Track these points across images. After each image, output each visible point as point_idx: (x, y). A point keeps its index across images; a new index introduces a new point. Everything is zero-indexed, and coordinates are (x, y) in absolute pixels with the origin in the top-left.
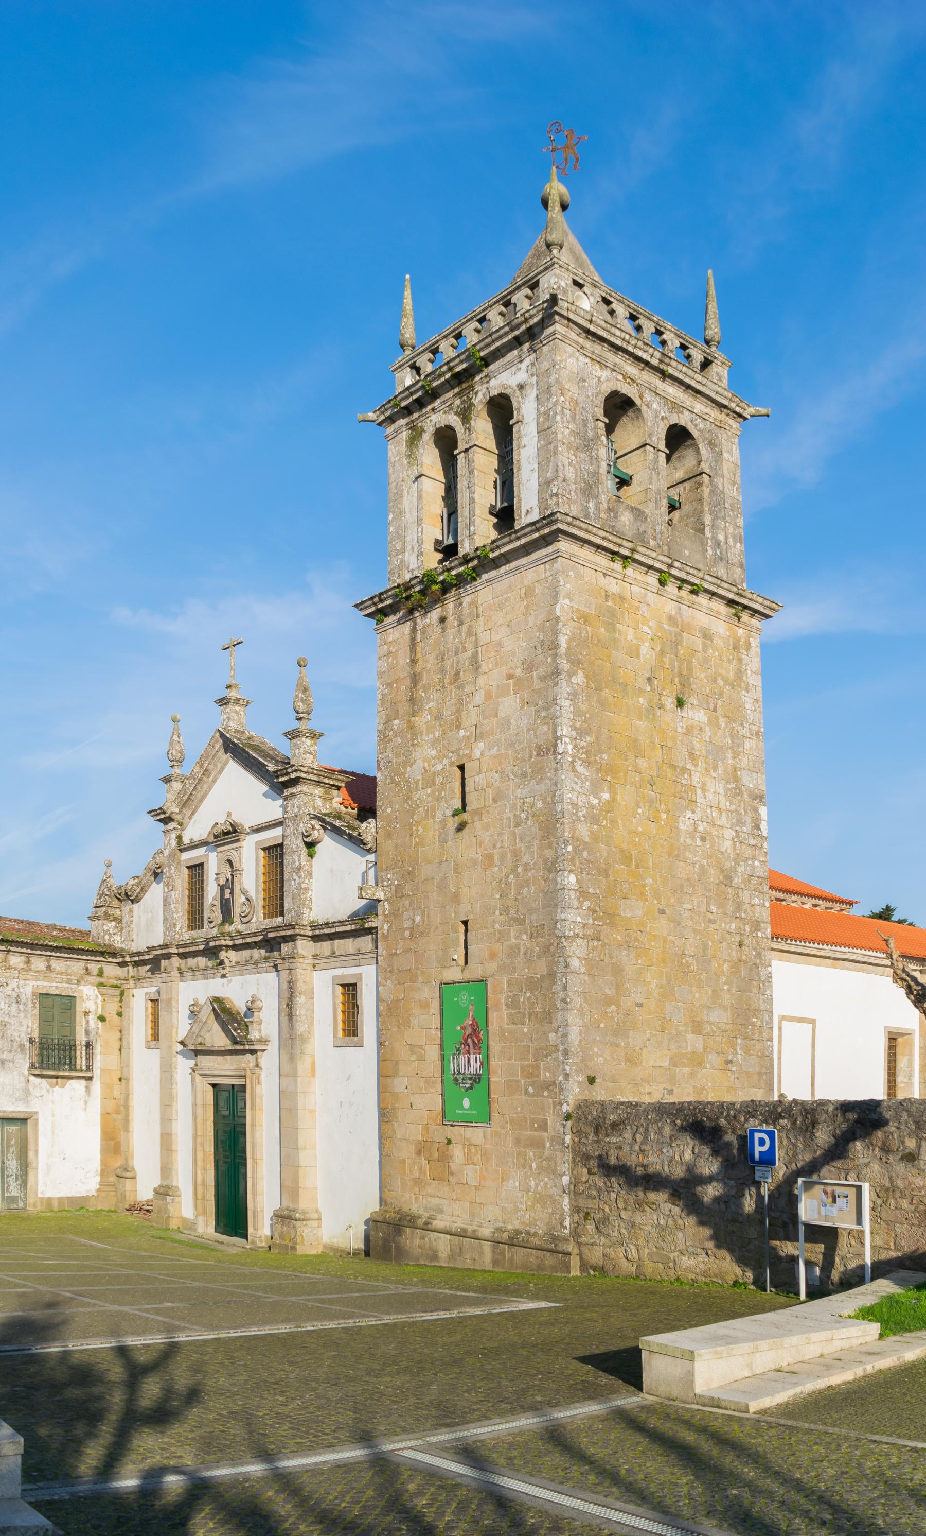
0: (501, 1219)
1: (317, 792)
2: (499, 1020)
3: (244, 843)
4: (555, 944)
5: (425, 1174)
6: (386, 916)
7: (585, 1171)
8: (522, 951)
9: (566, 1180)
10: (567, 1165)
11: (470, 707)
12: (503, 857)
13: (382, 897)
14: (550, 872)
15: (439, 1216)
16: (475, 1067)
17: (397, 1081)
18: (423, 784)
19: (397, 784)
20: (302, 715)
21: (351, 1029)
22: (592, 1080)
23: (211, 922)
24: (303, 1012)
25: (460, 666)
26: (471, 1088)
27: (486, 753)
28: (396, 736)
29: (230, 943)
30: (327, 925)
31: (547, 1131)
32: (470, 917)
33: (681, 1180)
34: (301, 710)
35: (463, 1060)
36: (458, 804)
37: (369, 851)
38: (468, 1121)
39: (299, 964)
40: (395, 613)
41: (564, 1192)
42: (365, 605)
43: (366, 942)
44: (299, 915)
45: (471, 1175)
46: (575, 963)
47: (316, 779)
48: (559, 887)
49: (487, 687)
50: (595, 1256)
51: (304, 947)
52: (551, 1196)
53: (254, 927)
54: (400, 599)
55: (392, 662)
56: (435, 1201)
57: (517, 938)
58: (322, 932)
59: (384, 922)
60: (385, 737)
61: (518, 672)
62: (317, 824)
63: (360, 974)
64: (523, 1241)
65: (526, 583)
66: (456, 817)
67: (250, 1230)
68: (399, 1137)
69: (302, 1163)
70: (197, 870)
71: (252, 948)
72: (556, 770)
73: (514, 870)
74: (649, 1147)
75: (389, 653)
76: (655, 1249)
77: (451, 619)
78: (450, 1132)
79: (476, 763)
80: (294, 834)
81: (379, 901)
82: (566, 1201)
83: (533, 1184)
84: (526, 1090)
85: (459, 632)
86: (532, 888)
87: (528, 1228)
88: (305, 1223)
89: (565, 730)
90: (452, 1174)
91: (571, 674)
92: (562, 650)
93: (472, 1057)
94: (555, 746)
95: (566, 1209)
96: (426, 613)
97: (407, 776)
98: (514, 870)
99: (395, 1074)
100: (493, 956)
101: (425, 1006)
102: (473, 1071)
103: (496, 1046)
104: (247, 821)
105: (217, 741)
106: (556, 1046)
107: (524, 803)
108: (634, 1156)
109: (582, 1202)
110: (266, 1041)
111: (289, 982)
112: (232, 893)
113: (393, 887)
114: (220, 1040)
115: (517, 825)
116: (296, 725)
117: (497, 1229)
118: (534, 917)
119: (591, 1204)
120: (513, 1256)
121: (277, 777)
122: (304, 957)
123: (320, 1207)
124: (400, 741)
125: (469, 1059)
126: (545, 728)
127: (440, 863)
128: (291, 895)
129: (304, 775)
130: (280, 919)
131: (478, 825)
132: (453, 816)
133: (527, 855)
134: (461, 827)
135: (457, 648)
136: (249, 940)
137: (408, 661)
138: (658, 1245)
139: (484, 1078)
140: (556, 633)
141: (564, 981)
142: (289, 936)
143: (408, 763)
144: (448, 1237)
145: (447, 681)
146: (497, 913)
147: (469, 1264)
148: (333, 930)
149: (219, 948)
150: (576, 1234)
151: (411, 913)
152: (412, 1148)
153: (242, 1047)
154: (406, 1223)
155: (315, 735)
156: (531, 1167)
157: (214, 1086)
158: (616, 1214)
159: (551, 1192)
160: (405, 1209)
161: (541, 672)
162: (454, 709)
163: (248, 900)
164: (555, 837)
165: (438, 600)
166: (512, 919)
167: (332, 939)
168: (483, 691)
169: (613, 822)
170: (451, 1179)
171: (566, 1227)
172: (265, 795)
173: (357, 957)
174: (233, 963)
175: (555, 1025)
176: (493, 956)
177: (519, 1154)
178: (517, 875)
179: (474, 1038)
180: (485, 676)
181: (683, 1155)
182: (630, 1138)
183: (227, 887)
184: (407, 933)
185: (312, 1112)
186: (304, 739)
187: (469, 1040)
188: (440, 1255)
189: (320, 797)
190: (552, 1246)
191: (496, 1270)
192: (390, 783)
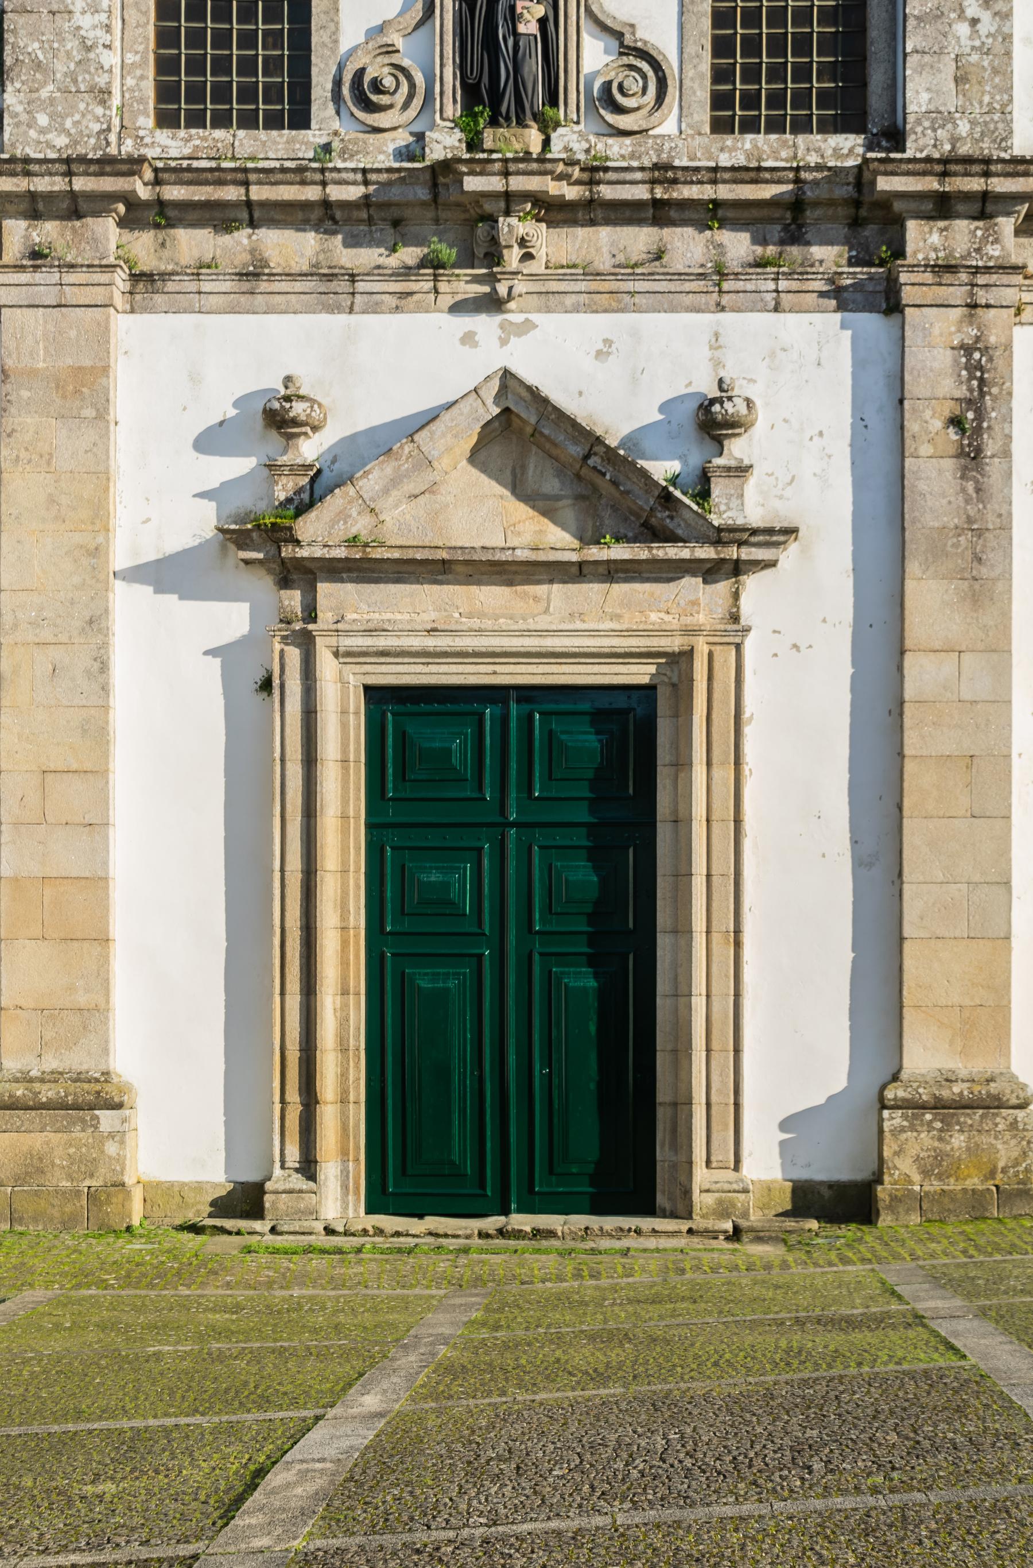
111: (967, 350)
128: (949, 68)
130: (844, 149)
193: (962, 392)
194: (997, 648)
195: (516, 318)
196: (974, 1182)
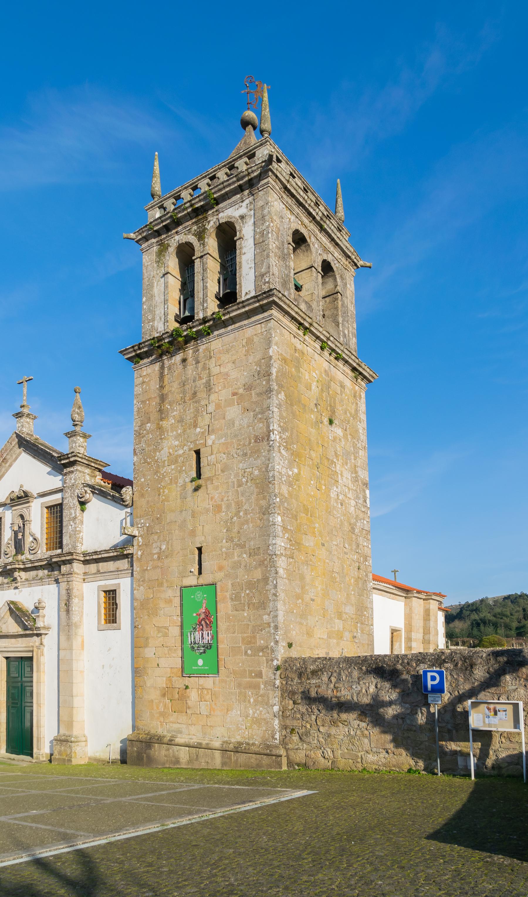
0: (226, 735)
1: (86, 471)
2: (225, 608)
3: (31, 504)
4: (268, 560)
5: (169, 708)
6: (140, 546)
7: (291, 702)
8: (243, 564)
9: (276, 708)
10: (277, 699)
11: (205, 413)
12: (228, 506)
13: (137, 535)
14: (264, 514)
15: (179, 735)
16: (207, 638)
17: (147, 650)
18: (168, 463)
19: (149, 463)
20: (77, 423)
22: (290, 645)
23: (7, 554)
24: (77, 609)
25: (197, 389)
26: (204, 652)
27: (216, 442)
28: (148, 434)
29: (22, 567)
30: (96, 553)
31: (262, 678)
32: (204, 545)
33: (367, 705)
34: (77, 420)
35: (198, 635)
36: (194, 475)
37: (126, 506)
38: (202, 674)
39: (74, 578)
40: (148, 357)
41: (275, 716)
42: (127, 351)
43: (124, 564)
44: (75, 547)
45: (204, 708)
46: (281, 571)
47: (86, 462)
48: (271, 523)
49: (217, 401)
50: (299, 756)
51: (78, 568)
52: (264, 719)
53: (39, 556)
54: (153, 348)
55: (146, 388)
56: (176, 726)
57: (239, 556)
58: (91, 557)
59: (138, 550)
60: (140, 434)
61: (241, 391)
62: (88, 490)
63: (119, 584)
64: (245, 749)
65: (247, 336)
66: (194, 483)
67: (35, 750)
68: (148, 685)
69: (75, 705)
71: (37, 570)
72: (269, 451)
73: (237, 514)
74: (341, 685)
75: (144, 382)
76: (346, 751)
77: (190, 360)
78: (187, 681)
79: (209, 449)
80: (71, 496)
81: (135, 537)
82: (276, 722)
83: (251, 712)
84: (246, 652)
85: (197, 368)
86: (251, 525)
87: (247, 741)
88: (77, 743)
89: (275, 426)
90: (189, 708)
91: (278, 393)
92: (274, 376)
93: (205, 633)
94: (269, 436)
95: (277, 727)
96: (172, 356)
97: (156, 458)
99: (146, 646)
100: (221, 568)
101: (169, 601)
102: (206, 641)
103: (222, 625)
104: (34, 490)
105: (14, 440)
106: (269, 624)
107: (245, 472)
108: (330, 692)
109: (288, 722)
110: (48, 628)
111: (67, 590)
112: (23, 536)
113: (145, 528)
114: (13, 628)
115: (239, 486)
116: (73, 428)
117: (224, 742)
118: (252, 543)
119: (295, 723)
120: (237, 759)
121: (60, 460)
122: (78, 574)
123: (86, 733)
124: (151, 437)
125: (202, 634)
126: (261, 425)
127: (181, 511)
128: (68, 535)
129: (79, 459)
130: (59, 551)
131: (210, 486)
132: (191, 481)
133: (247, 504)
134: (197, 489)
135: (195, 378)
136: (36, 564)
137: (158, 387)
138: (349, 748)
139: (214, 646)
140: (269, 366)
141: (275, 582)
142: (68, 560)
144: (187, 748)
145: (187, 398)
146: (224, 541)
147: (203, 765)
148: (100, 556)
149: (15, 569)
150: (284, 743)
151: (159, 544)
152: (158, 692)
153: (31, 632)
154: (155, 741)
155: (85, 436)
156: (249, 701)
157: (7, 658)
158: (316, 729)
159: (265, 716)
160: (153, 731)
161: (258, 390)
162: (192, 415)
163: (35, 539)
164: (268, 493)
165: (181, 348)
166: (235, 544)
167: (97, 563)
168: (214, 404)
170: (188, 711)
171: (276, 739)
172: (49, 473)
173: (117, 573)
174: (23, 580)
175: (268, 610)
176: (221, 568)
177: (240, 693)
178: (240, 517)
179: (207, 620)
180: (216, 394)
181: (368, 688)
182: (327, 679)
184: (156, 556)
185: (82, 672)
186: (79, 438)
187: (203, 622)
188: (181, 760)
189: (88, 474)
190: (268, 752)
191: (225, 768)
192: (143, 463)
193: (67, 599)
194: (71, 649)
195: (20, 589)
196: (64, 757)
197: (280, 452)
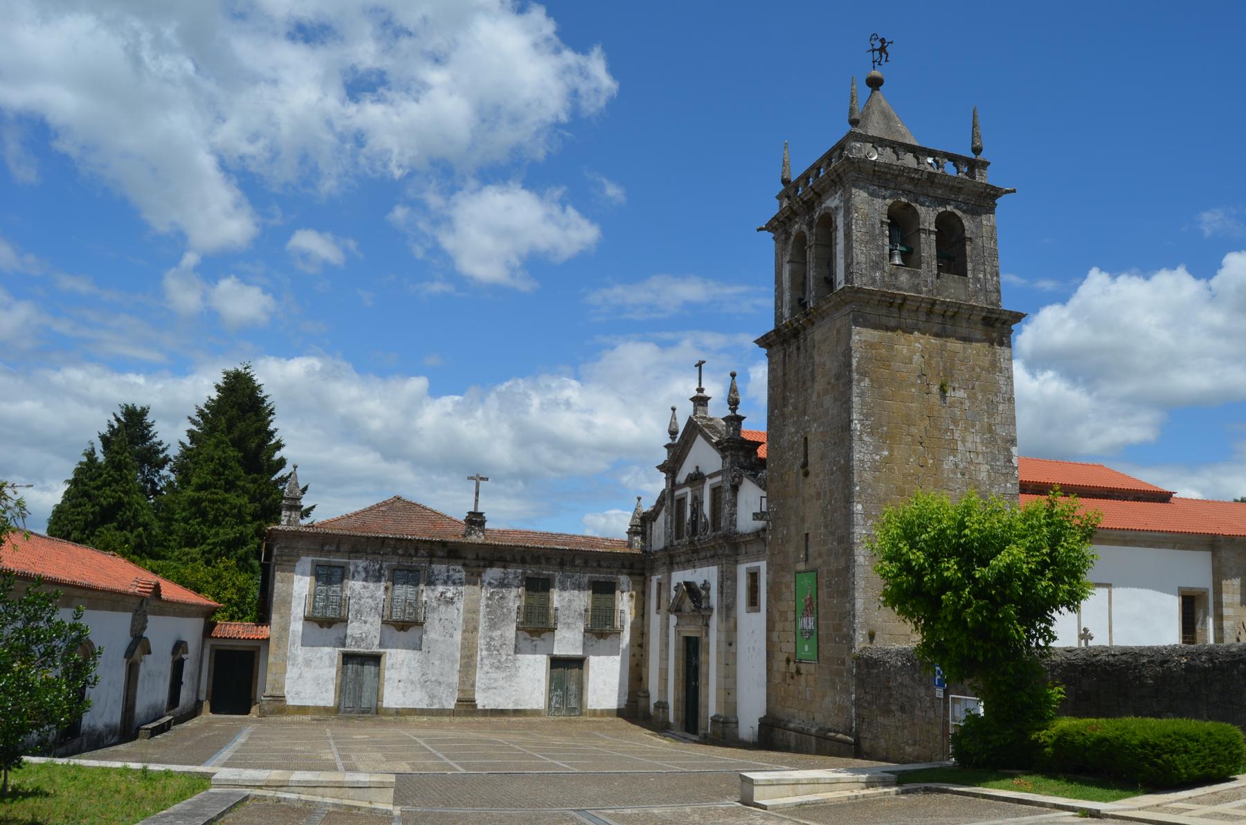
21: (753, 602)
70: (681, 501)
73: (830, 503)
98: (830, 503)
143: (781, 436)
169: (891, 470)
176: (820, 555)
183: (696, 511)
197: (861, 440)
